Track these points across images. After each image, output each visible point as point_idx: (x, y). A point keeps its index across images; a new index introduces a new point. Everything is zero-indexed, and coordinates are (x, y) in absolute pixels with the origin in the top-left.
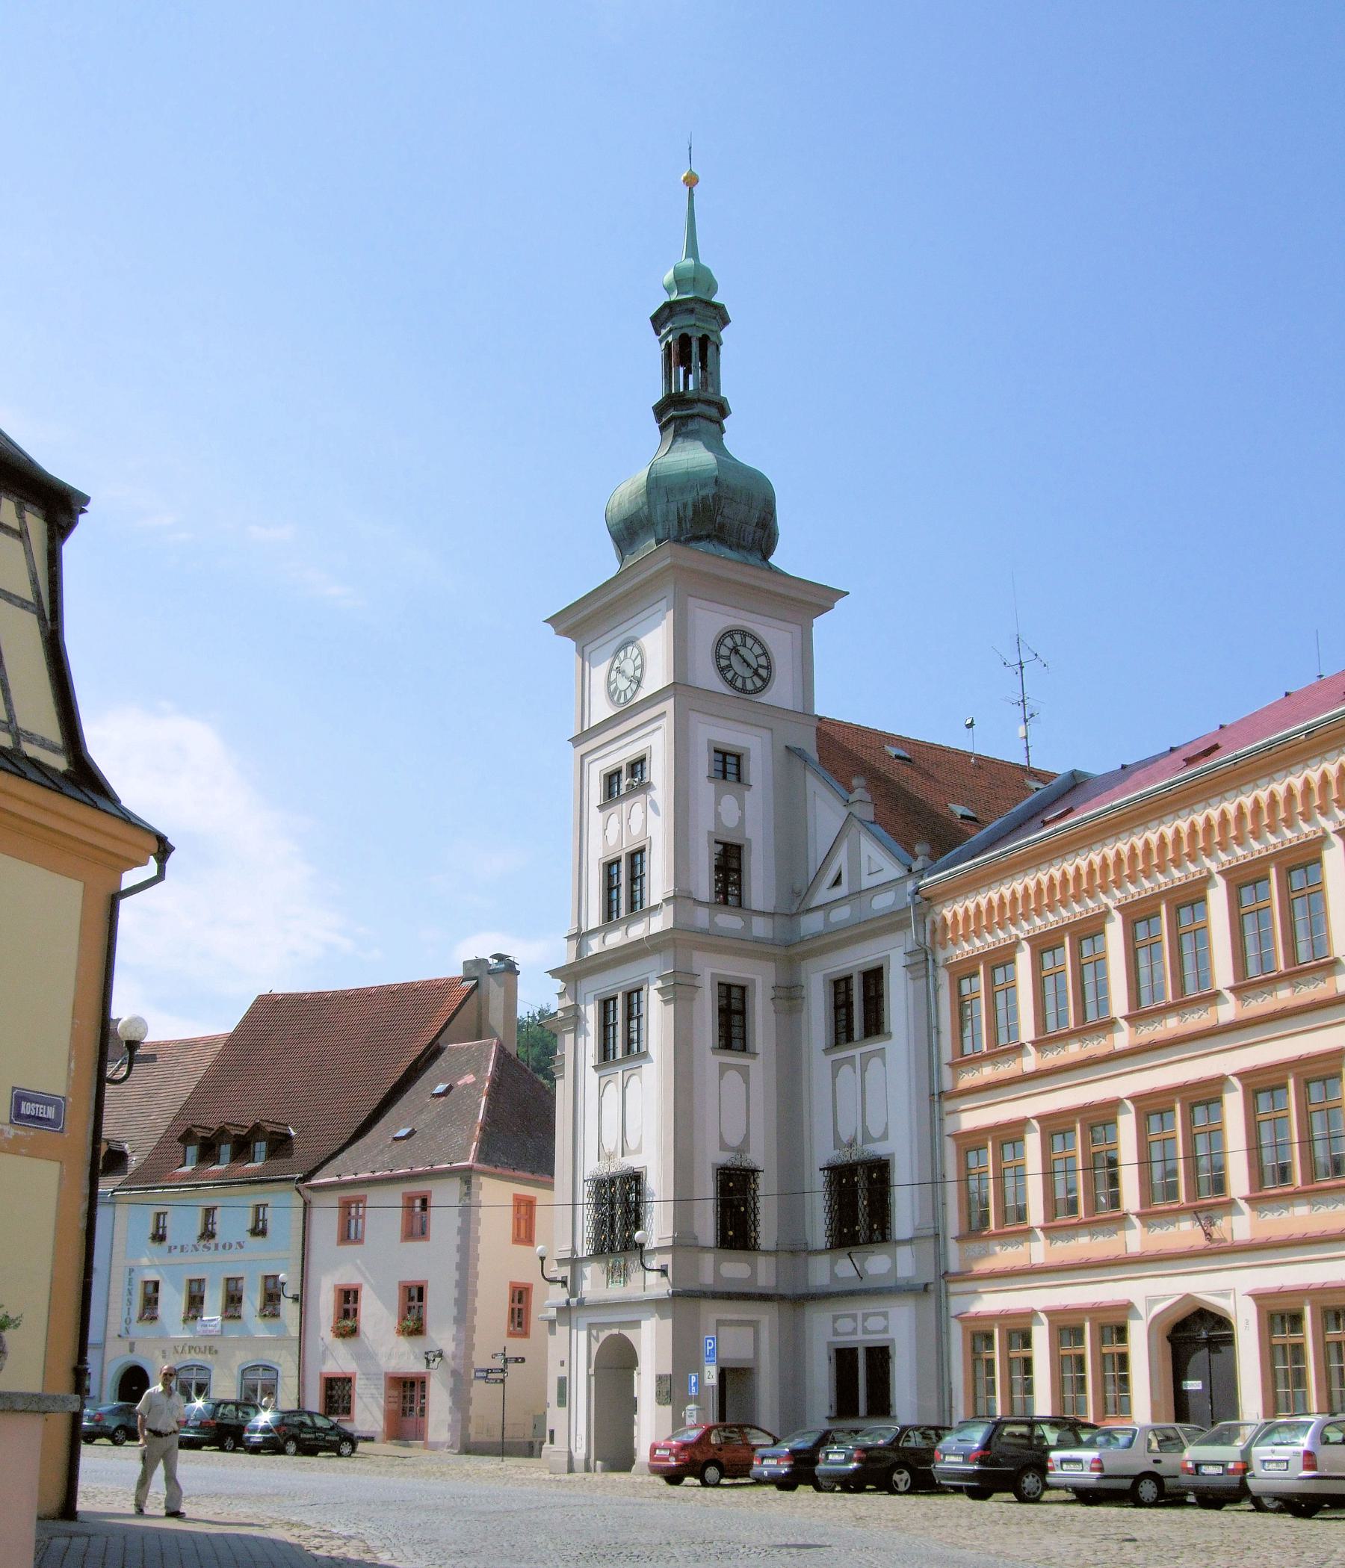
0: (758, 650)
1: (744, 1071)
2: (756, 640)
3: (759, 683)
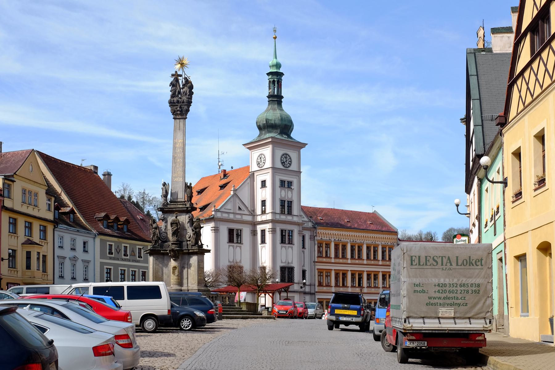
1: (292, 248)
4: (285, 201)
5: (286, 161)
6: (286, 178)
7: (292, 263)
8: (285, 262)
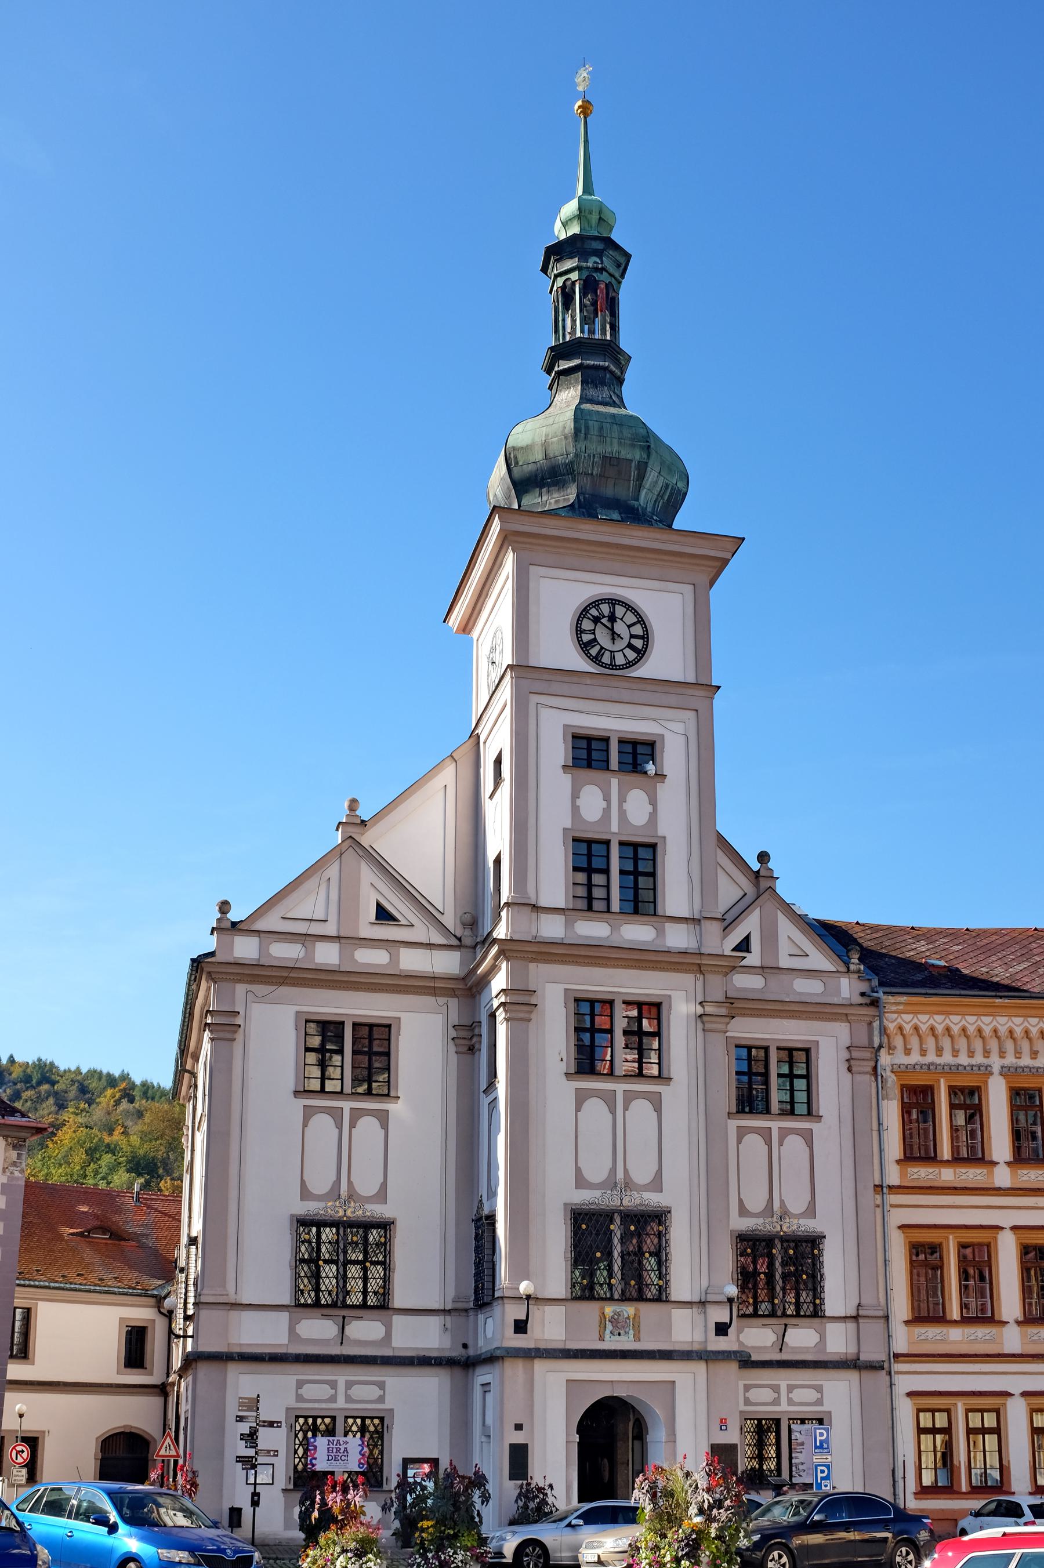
0: (631, 618)
2: (629, 607)
3: (631, 655)
4: (607, 843)
5: (609, 636)
6: (616, 722)
7: (657, 1184)
8: (610, 1183)
